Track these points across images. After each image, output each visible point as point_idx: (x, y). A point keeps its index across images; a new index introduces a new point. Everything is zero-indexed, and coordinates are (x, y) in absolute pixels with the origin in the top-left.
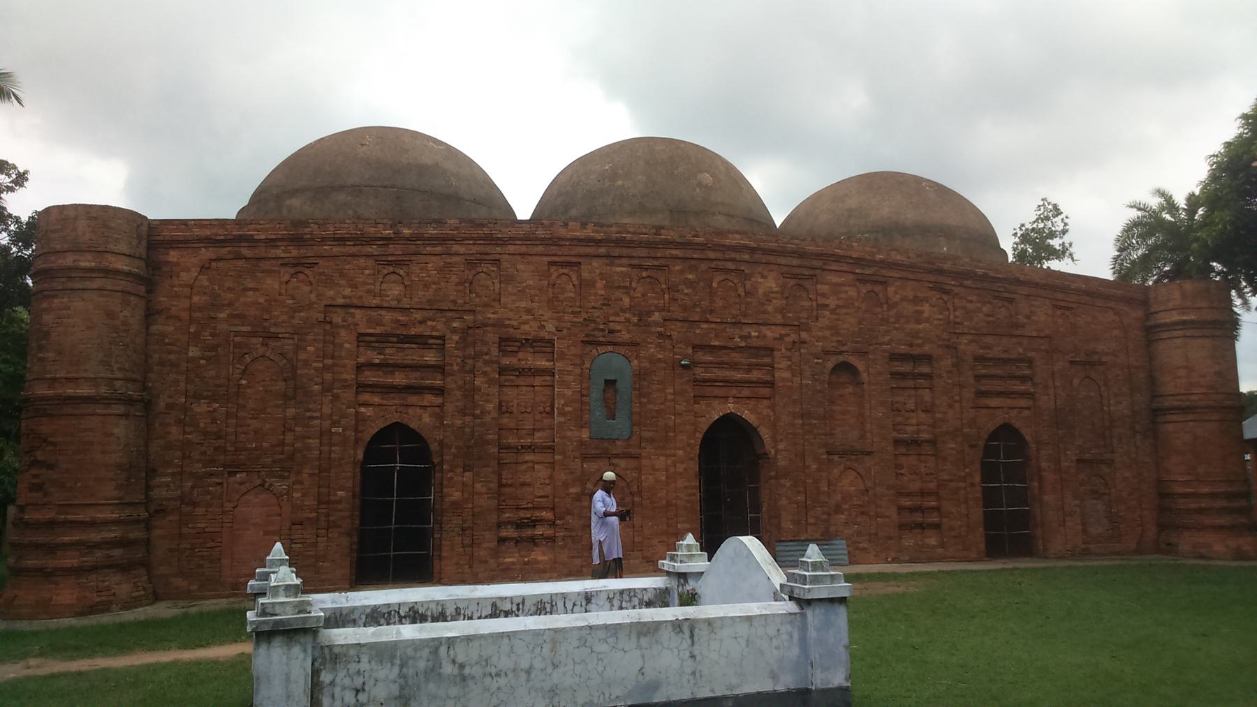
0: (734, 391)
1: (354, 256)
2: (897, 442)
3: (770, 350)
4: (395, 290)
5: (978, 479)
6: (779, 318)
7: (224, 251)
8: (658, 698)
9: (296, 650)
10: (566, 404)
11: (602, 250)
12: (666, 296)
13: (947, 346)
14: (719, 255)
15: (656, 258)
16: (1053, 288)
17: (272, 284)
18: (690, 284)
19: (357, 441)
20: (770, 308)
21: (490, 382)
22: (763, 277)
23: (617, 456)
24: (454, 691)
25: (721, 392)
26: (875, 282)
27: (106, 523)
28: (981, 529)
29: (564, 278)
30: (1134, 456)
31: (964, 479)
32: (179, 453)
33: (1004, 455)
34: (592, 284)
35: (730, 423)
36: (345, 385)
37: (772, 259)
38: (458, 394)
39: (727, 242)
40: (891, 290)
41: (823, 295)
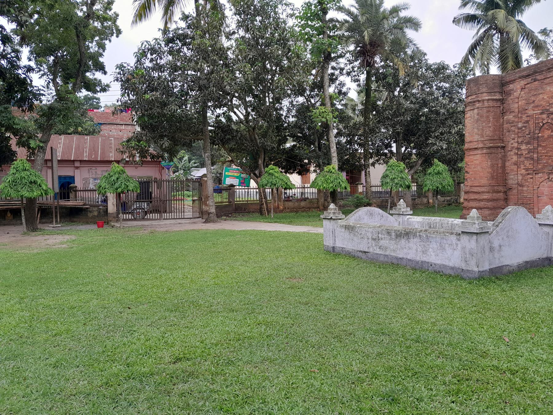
7: (530, 79)
27: (483, 192)
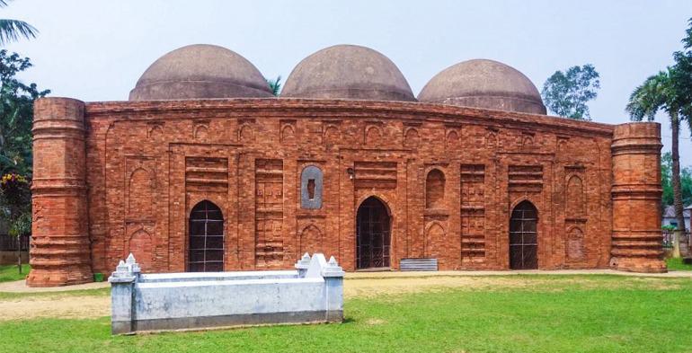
0: (376, 185)
1: (183, 119)
2: (463, 210)
3: (395, 164)
4: (202, 136)
5: (507, 229)
6: (401, 147)
7: (120, 118)
8: (265, 311)
9: (126, 289)
10: (289, 191)
11: (307, 113)
12: (341, 137)
13: (495, 161)
14: (370, 115)
15: (336, 117)
16: (558, 127)
17: (143, 132)
18: (354, 130)
19: (186, 209)
20: (396, 142)
21: (251, 180)
22: (393, 125)
23: (314, 217)
24: (184, 306)
25: (370, 185)
26: (455, 127)
28: (507, 255)
29: (288, 128)
30: (599, 217)
31: (499, 229)
32: (103, 214)
33: (522, 217)
34: (302, 131)
35: (372, 198)
36: (180, 182)
37: (398, 115)
38: (235, 186)
39: (374, 107)
40: (464, 130)
41: (426, 134)
